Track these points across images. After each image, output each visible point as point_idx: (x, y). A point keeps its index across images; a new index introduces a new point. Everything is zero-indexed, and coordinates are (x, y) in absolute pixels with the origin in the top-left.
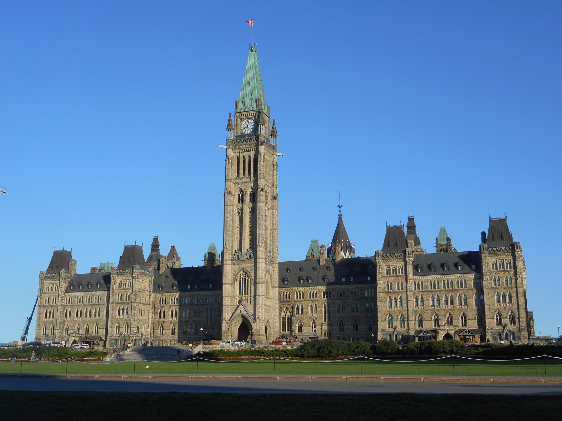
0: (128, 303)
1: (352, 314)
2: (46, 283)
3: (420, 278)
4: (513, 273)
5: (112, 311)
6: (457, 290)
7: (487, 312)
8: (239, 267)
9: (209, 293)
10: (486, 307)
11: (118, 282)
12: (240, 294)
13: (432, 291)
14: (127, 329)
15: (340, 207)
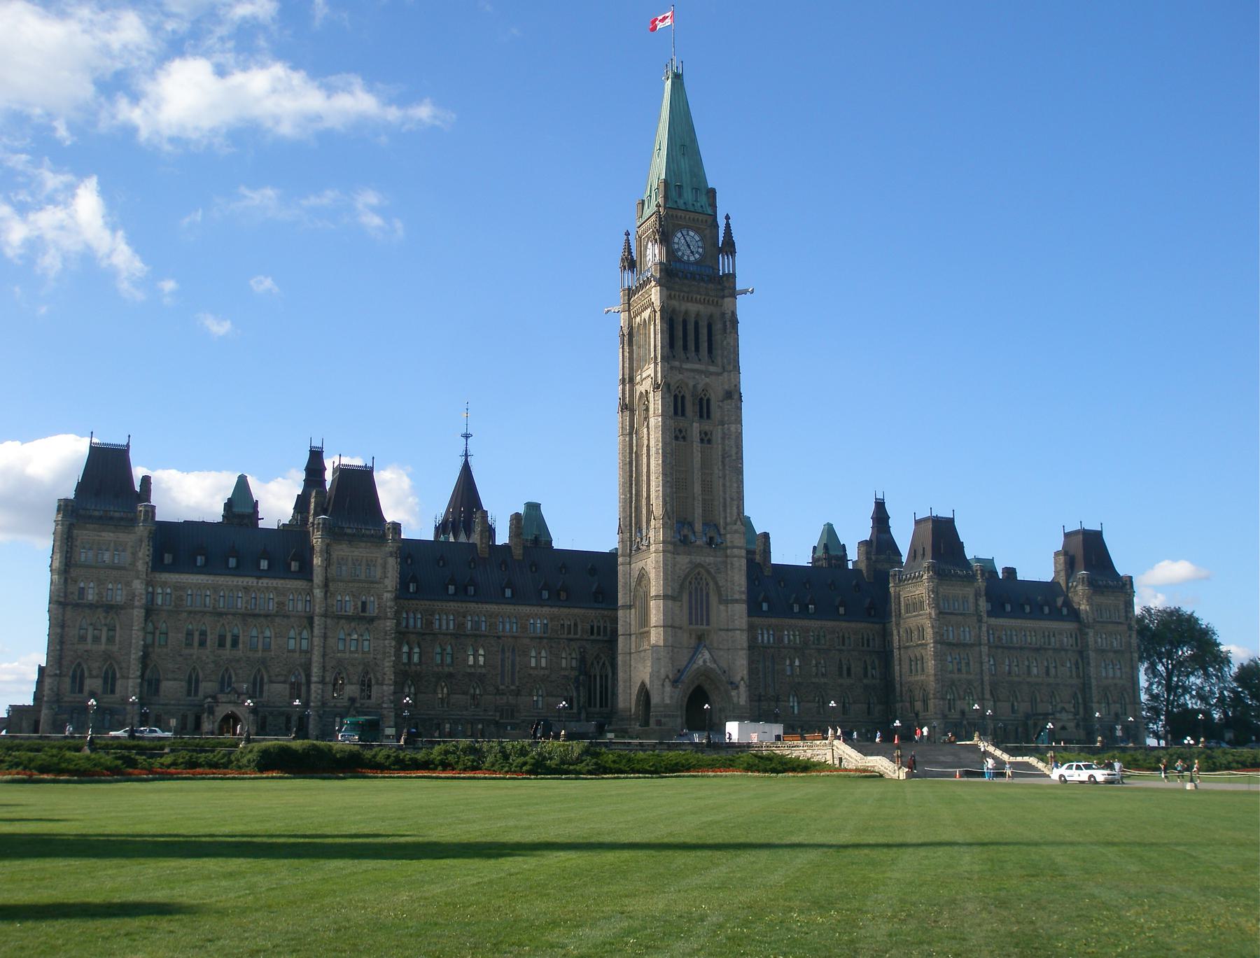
0: (371, 620)
1: (814, 680)
2: (85, 535)
3: (993, 621)
4: (1125, 627)
5: (325, 637)
6: (1046, 649)
7: (1094, 691)
8: (690, 562)
9: (509, 609)
10: (1094, 682)
11: (334, 555)
12: (691, 623)
13: (1009, 648)
14: (366, 685)
15: (467, 436)
